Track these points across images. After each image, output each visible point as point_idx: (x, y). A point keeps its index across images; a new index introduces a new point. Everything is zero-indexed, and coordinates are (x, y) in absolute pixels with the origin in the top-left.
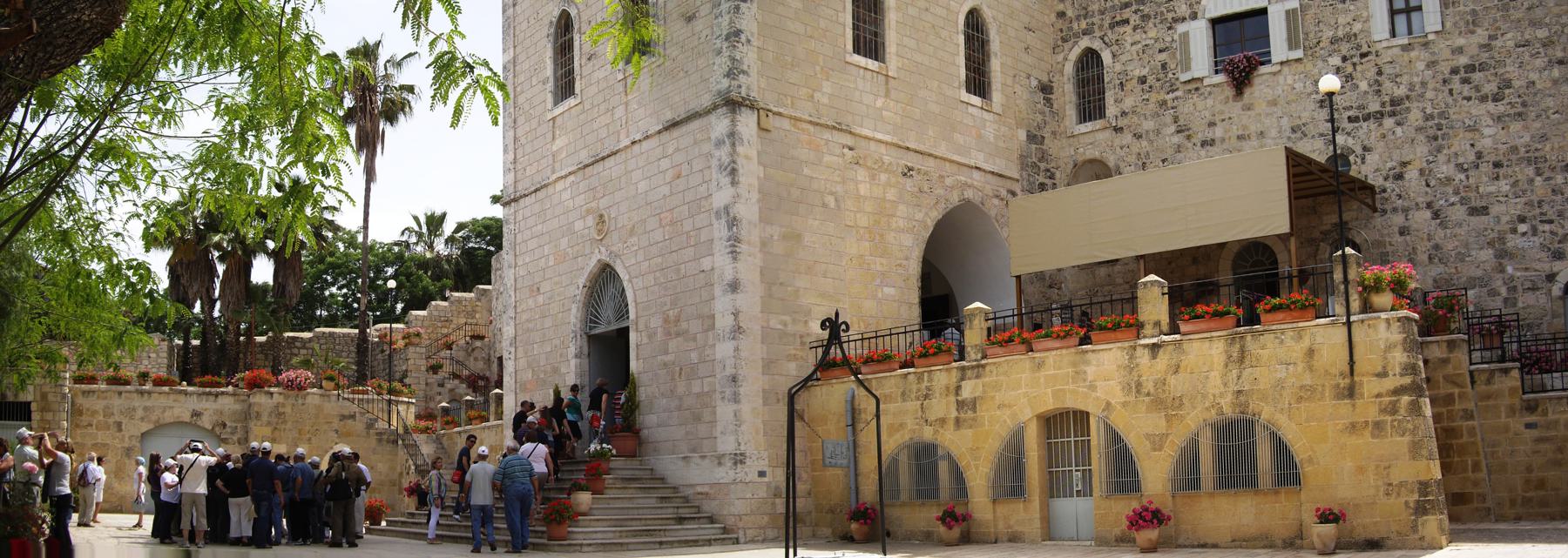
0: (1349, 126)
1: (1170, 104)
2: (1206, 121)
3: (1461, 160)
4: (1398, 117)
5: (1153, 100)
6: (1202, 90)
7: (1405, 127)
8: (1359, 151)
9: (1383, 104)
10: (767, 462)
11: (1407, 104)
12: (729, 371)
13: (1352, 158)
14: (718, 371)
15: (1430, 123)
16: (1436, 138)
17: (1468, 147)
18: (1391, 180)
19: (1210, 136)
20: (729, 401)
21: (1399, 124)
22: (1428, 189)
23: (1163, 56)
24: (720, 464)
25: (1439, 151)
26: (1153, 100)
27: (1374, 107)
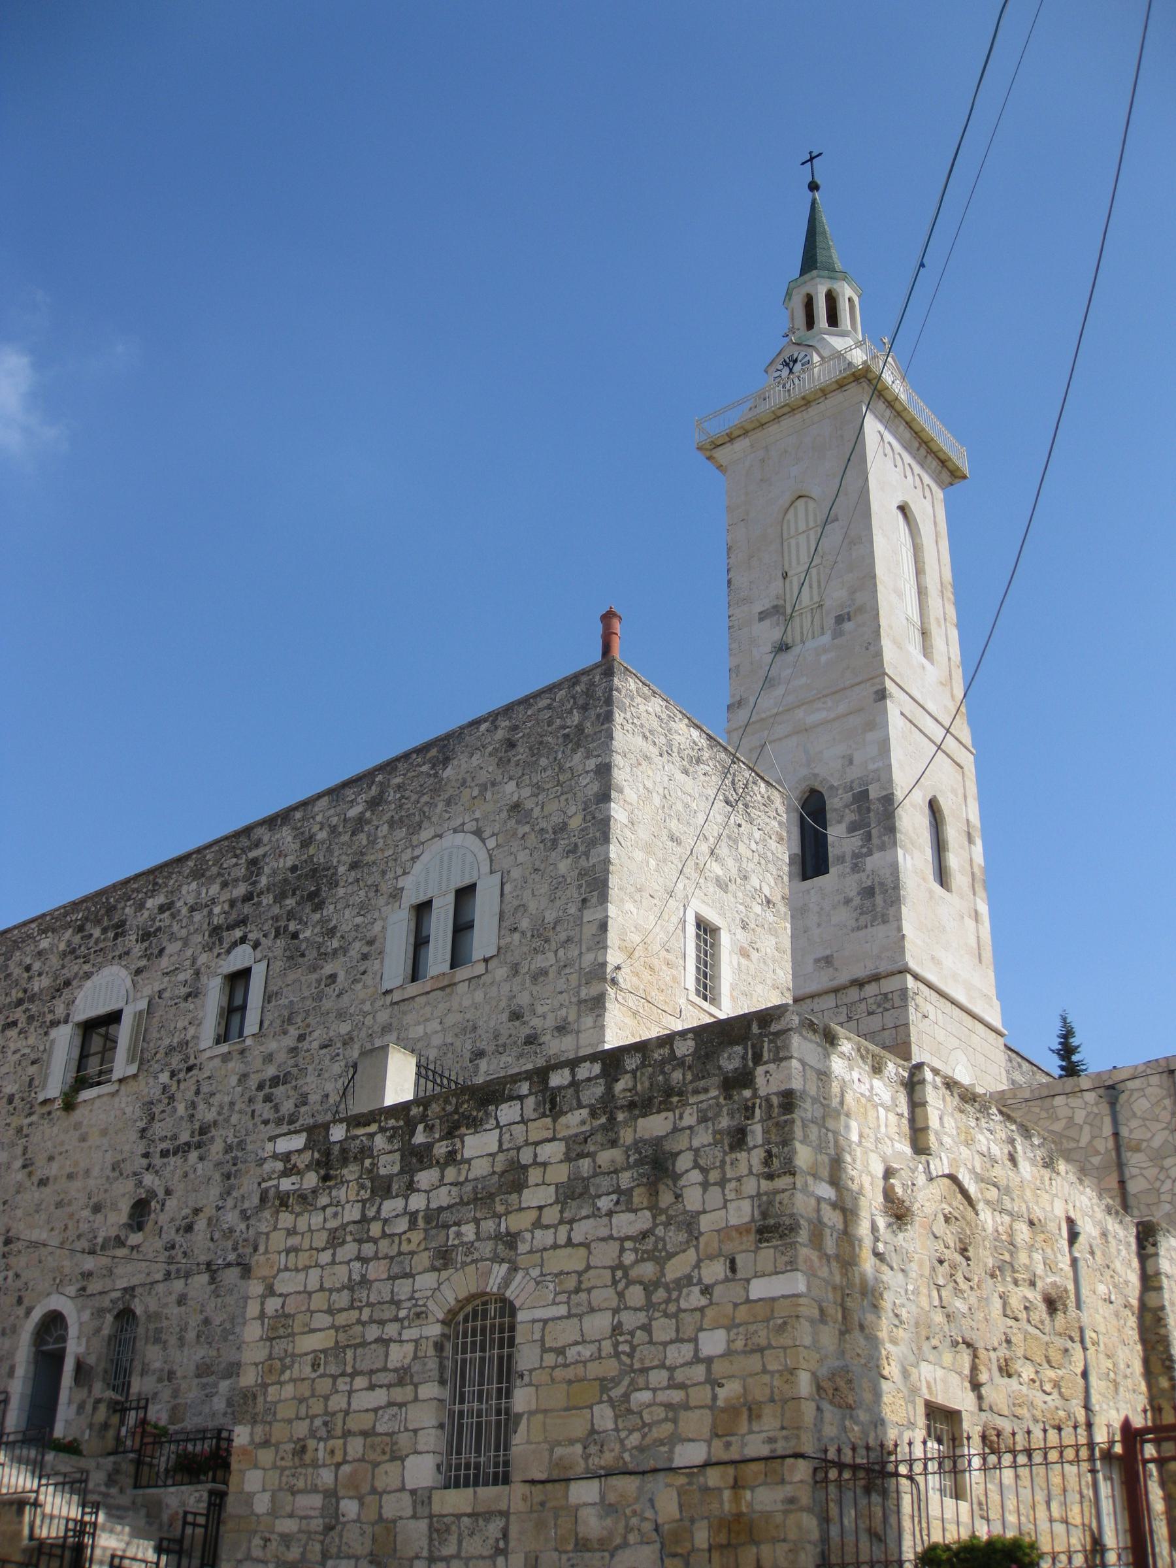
0: (157, 1161)
1: (25, 1131)
2: (45, 1155)
3: (246, 1205)
4: (201, 1150)
5: (13, 1125)
6: (53, 1115)
7: (206, 1163)
8: (161, 1194)
9: (193, 1132)
11: (213, 1132)
13: (153, 1204)
15: (228, 1157)
16: (228, 1176)
17: (256, 1185)
18: (181, 1232)
19: (46, 1172)
21: (201, 1159)
22: (211, 1244)
23: (32, 1070)
25: (229, 1194)
26: (13, 1125)
27: (185, 1137)
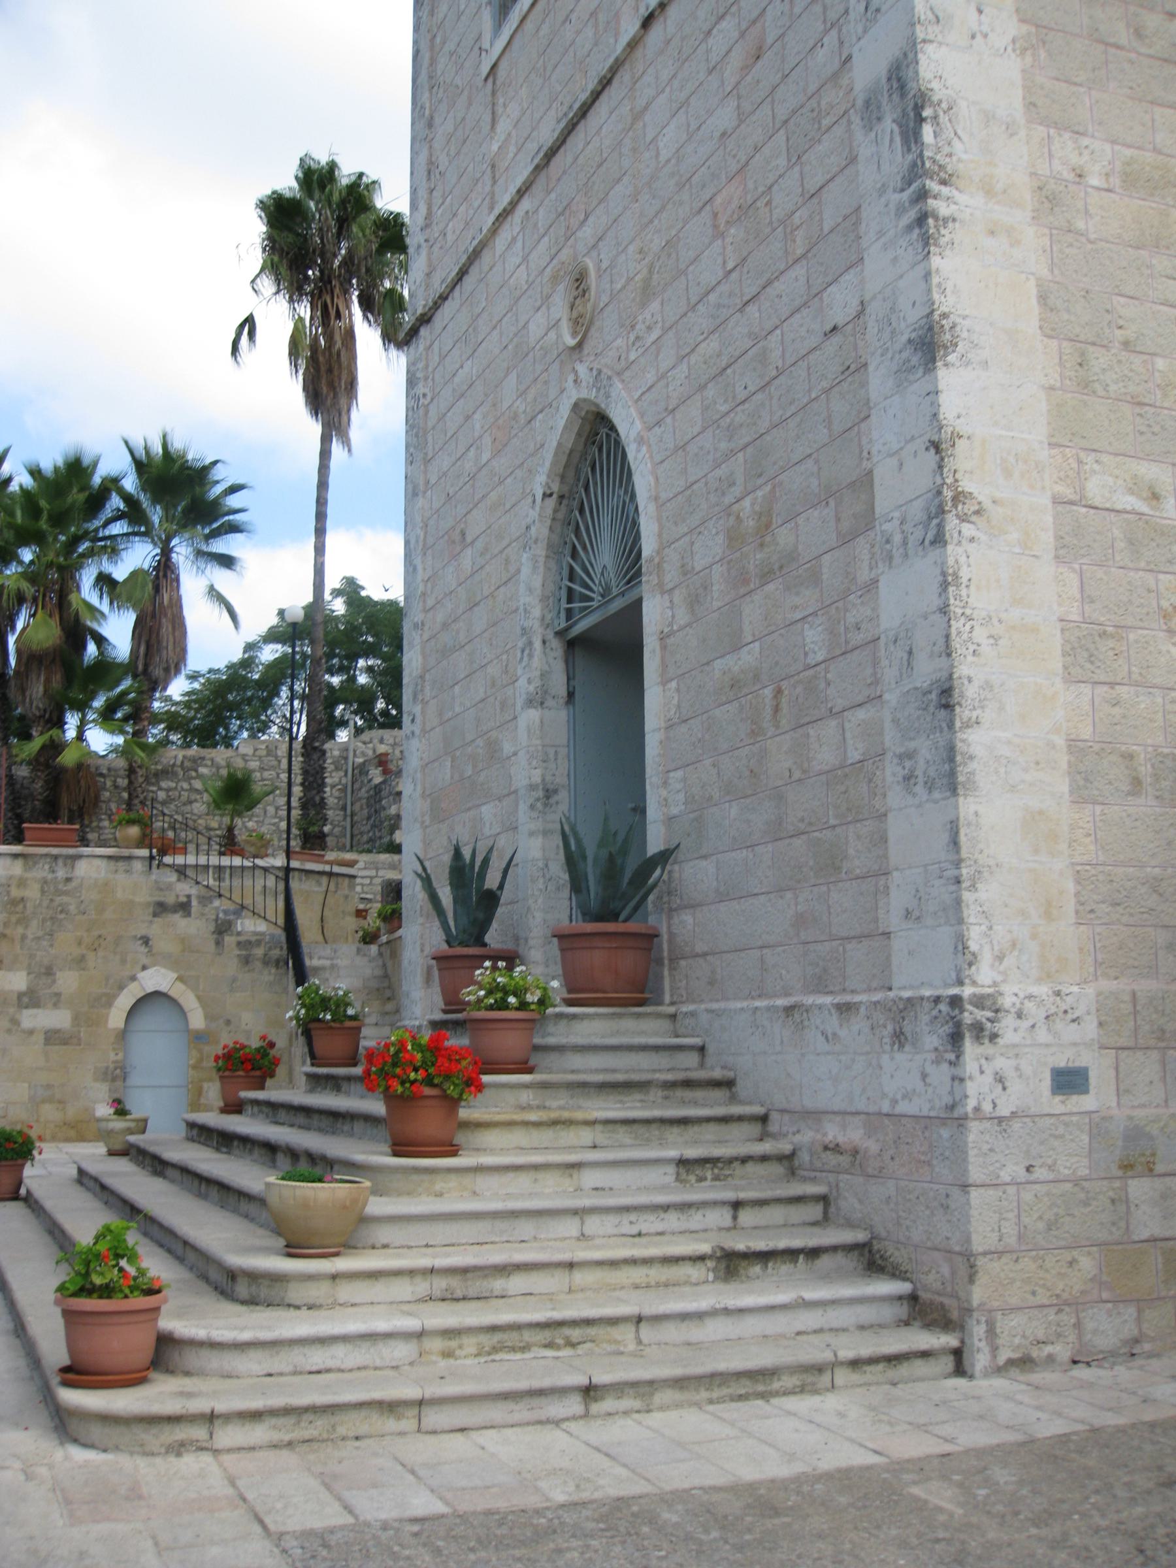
10: (1090, 1029)
12: (926, 671)
14: (889, 674)
20: (930, 786)
24: (899, 1038)
